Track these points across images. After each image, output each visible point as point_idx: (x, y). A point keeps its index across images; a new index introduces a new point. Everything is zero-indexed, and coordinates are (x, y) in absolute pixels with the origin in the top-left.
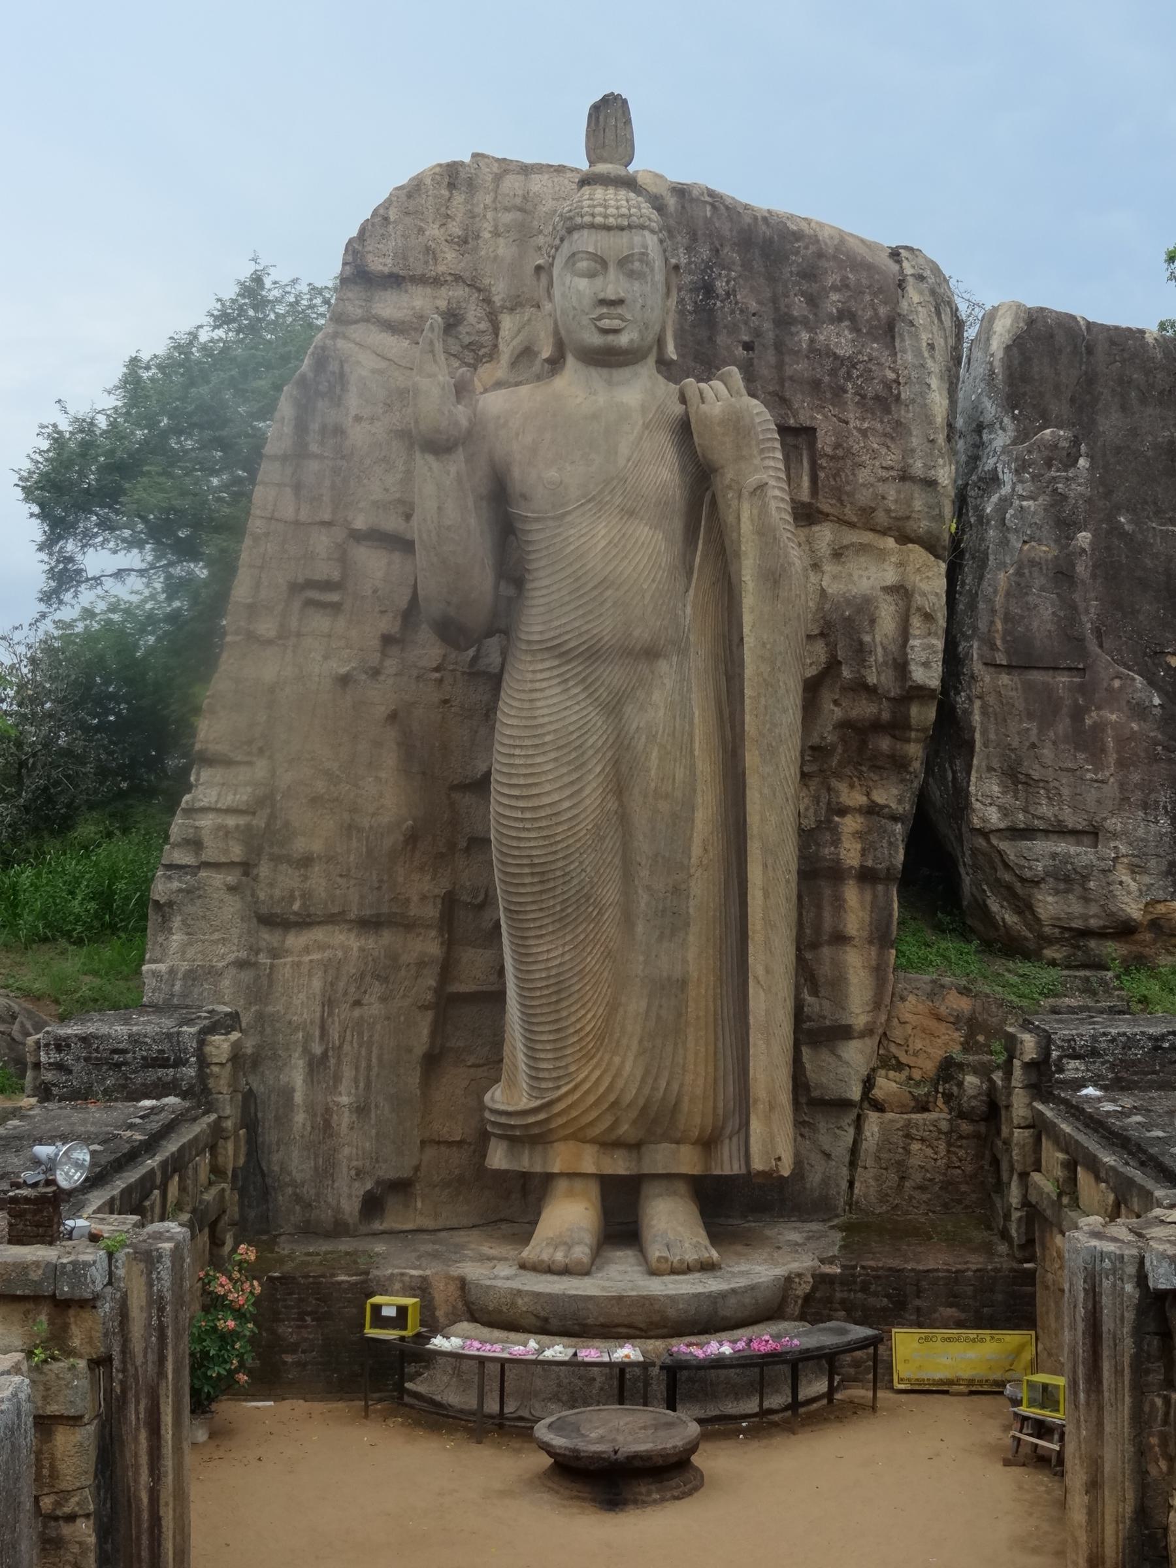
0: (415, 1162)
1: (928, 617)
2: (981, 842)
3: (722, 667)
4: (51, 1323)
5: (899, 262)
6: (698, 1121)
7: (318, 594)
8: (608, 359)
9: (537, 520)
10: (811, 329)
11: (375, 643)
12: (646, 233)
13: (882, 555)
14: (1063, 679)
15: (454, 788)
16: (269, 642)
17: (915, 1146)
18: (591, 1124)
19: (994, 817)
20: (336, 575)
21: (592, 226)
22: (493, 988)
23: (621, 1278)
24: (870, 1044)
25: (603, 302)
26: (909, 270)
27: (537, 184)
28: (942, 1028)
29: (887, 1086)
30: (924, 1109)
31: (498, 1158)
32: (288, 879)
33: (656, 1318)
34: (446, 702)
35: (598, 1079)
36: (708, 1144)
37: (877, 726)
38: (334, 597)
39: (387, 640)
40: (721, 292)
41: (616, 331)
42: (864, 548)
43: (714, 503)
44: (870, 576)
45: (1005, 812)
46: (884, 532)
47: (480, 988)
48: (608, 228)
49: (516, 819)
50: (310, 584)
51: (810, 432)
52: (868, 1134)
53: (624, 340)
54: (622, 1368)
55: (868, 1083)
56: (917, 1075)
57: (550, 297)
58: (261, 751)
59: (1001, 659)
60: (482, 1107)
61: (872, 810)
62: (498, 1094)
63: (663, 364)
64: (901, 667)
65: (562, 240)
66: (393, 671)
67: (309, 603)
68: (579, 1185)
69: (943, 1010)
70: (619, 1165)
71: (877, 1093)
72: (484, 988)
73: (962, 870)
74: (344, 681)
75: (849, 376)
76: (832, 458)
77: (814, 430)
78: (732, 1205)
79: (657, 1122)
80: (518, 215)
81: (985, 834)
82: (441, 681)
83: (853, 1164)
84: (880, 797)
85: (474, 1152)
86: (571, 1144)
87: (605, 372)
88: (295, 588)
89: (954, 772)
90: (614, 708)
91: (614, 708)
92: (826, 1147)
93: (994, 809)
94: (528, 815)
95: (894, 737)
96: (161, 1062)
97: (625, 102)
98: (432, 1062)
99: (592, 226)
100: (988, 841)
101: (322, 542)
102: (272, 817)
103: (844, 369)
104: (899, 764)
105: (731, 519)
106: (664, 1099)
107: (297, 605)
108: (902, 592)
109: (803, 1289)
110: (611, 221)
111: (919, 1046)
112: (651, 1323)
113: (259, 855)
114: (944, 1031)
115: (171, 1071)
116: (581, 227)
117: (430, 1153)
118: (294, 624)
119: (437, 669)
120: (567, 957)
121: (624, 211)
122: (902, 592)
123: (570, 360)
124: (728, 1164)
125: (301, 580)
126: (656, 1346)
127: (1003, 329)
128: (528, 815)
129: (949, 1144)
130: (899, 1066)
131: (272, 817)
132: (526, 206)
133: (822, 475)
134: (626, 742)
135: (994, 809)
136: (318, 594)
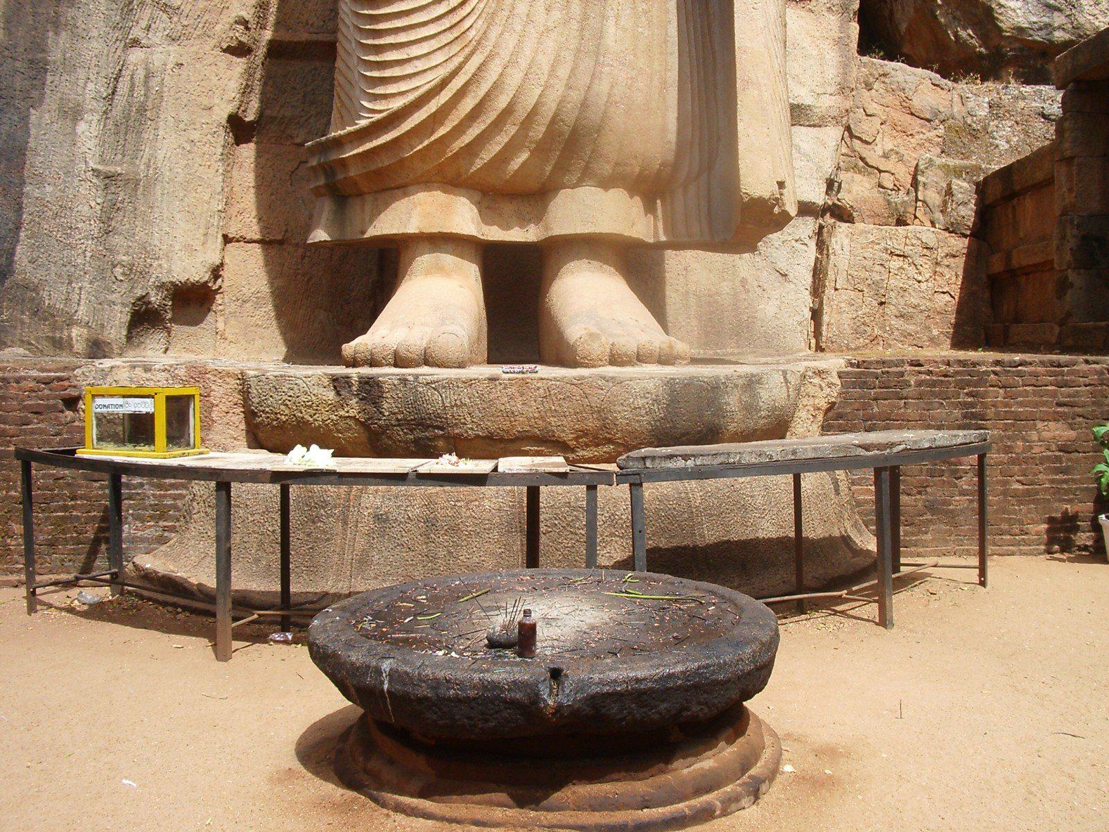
17: (896, 263)
24: (833, 134)
29: (856, 190)
30: (901, 222)
33: (591, 423)
35: (481, 68)
47: (314, 37)
52: (837, 247)
55: (831, 185)
56: (888, 181)
69: (917, 103)
71: (846, 198)
83: (817, 289)
85: (303, 257)
92: (782, 265)
106: (584, 105)
109: (824, 394)
111: (889, 146)
112: (585, 433)
114: (918, 129)
130: (867, 167)
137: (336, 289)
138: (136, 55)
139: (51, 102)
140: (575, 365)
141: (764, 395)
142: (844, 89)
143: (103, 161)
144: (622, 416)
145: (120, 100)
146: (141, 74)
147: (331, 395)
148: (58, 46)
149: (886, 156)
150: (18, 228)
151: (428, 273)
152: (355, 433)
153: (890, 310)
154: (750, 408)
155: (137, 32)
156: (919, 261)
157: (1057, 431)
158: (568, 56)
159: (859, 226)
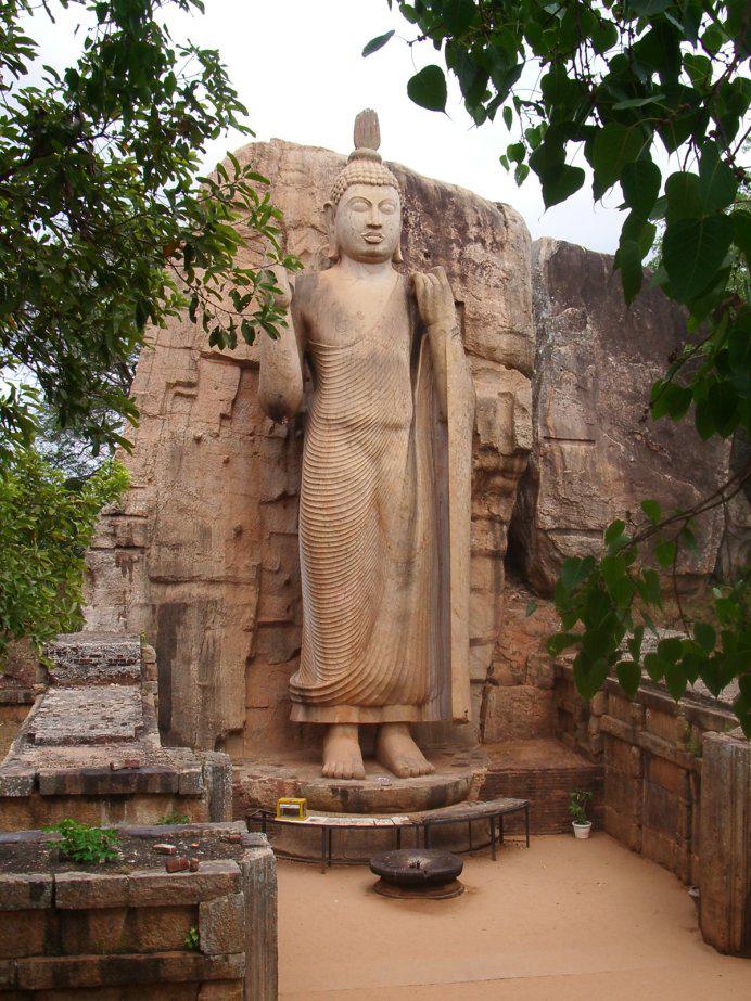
0: (244, 718)
1: (524, 410)
2: (541, 535)
3: (429, 435)
4: (174, 808)
5: (503, 212)
6: (417, 692)
7: (185, 389)
8: (371, 259)
9: (333, 349)
10: (461, 247)
11: (217, 419)
12: (392, 188)
13: (499, 374)
14: (583, 447)
15: (261, 503)
16: (155, 417)
17: (516, 704)
18: (358, 694)
19: (548, 523)
20: (194, 379)
21: (365, 183)
22: (286, 618)
23: (376, 782)
24: (490, 648)
25: (370, 226)
26: (508, 217)
27: (309, 156)
28: (528, 639)
29: (501, 671)
30: (520, 683)
31: (299, 716)
32: (168, 555)
34: (256, 454)
36: (420, 705)
37: (494, 472)
38: (192, 391)
39: (223, 417)
40: (412, 223)
41: (376, 243)
42: (489, 370)
43: (428, 341)
44: (492, 388)
45: (556, 519)
46: (499, 362)
48: (372, 184)
49: (319, 521)
50: (178, 384)
51: (463, 303)
53: (380, 248)
54: (397, 829)
55: (490, 670)
57: (333, 223)
58: (149, 480)
59: (552, 434)
60: (289, 686)
61: (492, 519)
62: (297, 679)
63: (395, 262)
64: (511, 438)
65: (345, 190)
66: (226, 435)
67: (178, 394)
68: (349, 730)
70: (371, 718)
71: (496, 675)
72: (279, 619)
73: (529, 551)
74: (198, 440)
75: (481, 274)
76: (473, 320)
77: (463, 303)
78: (435, 739)
79: (393, 693)
80: (299, 175)
81: (545, 532)
82: (253, 441)
84: (495, 511)
86: (345, 707)
87: (370, 267)
88: (169, 386)
89: (526, 497)
90: (376, 458)
91: (376, 458)
93: (549, 518)
94: (327, 519)
95: (504, 477)
96: (124, 663)
97: (376, 115)
98: (250, 661)
99: (365, 183)
100: (547, 536)
101: (184, 359)
102: (157, 520)
103: (479, 271)
104: (505, 493)
105: (440, 352)
107: (171, 395)
108: (509, 396)
109: (480, 782)
110: (374, 181)
111: (515, 648)
113: (150, 542)
115: (127, 668)
116: (353, 183)
117: (251, 713)
118: (169, 408)
119: (251, 435)
120: (347, 600)
121: (381, 175)
122: (509, 396)
123: (346, 261)
124: (431, 714)
125: (173, 381)
126: (419, 816)
127: (544, 255)
128: (327, 519)
129: (534, 703)
131: (157, 520)
132: (304, 169)
133: (467, 328)
134: (383, 478)
135: (549, 518)
136: (185, 389)
137: (309, 742)
138: (209, 633)
139: (179, 656)
140: (399, 776)
141: (460, 787)
142: (496, 627)
143: (200, 680)
144: (418, 798)
145: (204, 653)
146: (211, 641)
147: (331, 794)
148: (180, 632)
149: (514, 654)
150: (171, 709)
151: (341, 737)
152: (340, 805)
153: (514, 725)
154: (455, 792)
155: (208, 625)
156: (527, 702)
157: (559, 792)
158: (394, 664)
159: (502, 688)
